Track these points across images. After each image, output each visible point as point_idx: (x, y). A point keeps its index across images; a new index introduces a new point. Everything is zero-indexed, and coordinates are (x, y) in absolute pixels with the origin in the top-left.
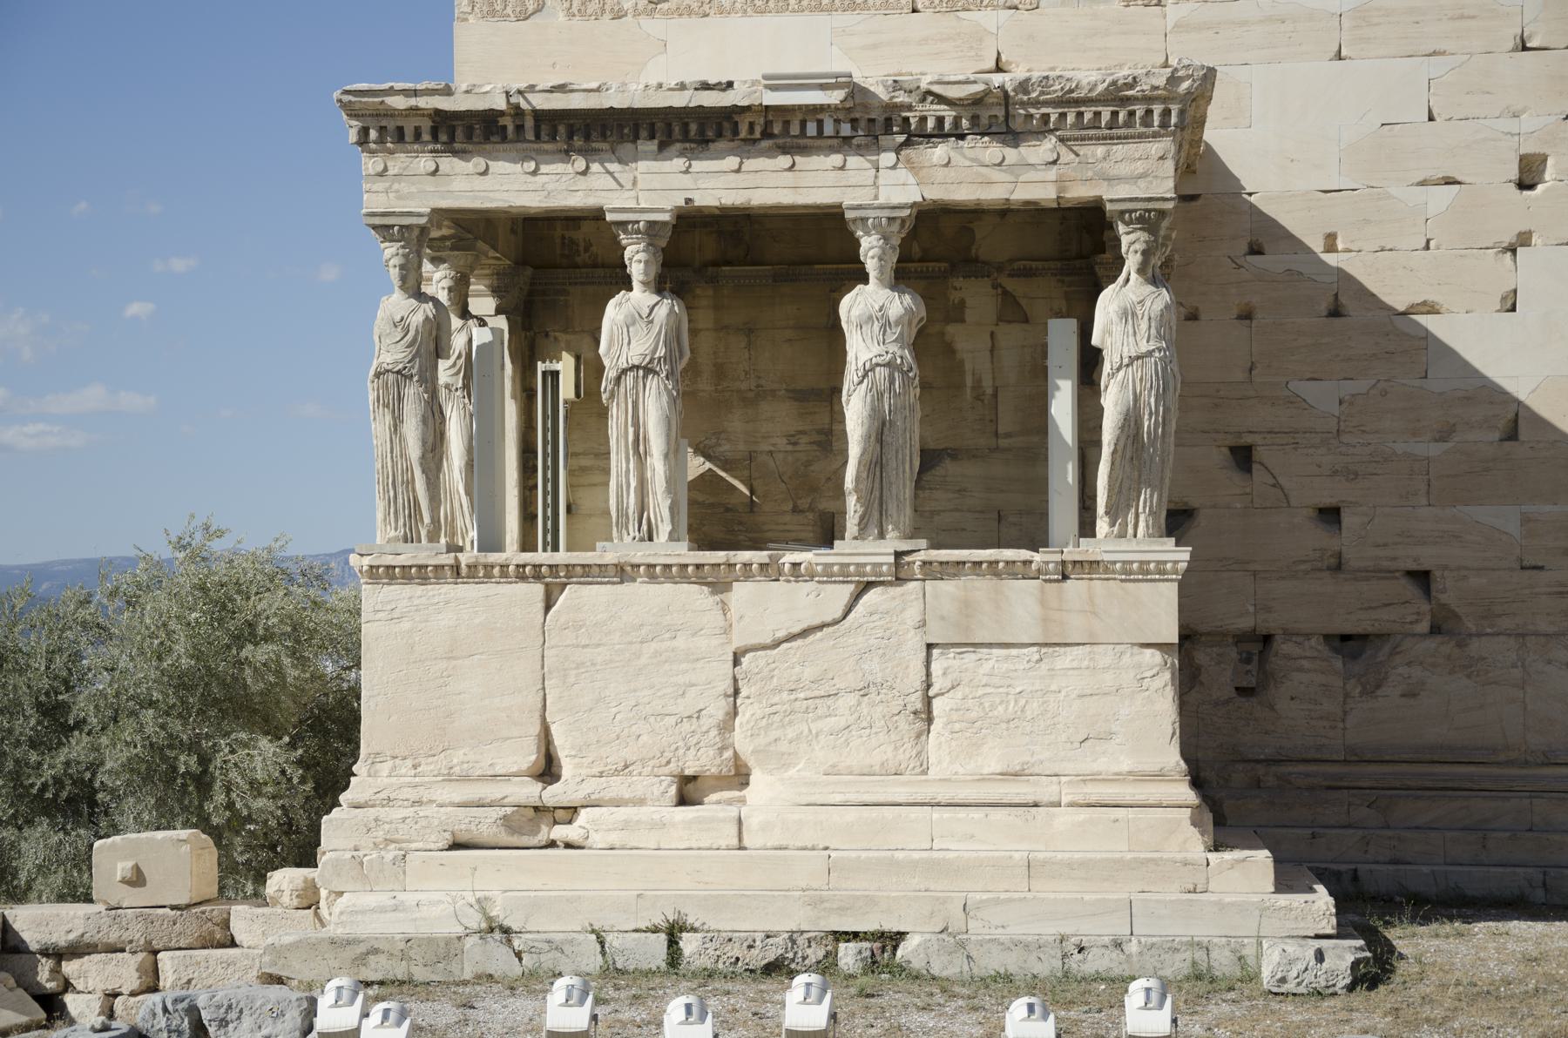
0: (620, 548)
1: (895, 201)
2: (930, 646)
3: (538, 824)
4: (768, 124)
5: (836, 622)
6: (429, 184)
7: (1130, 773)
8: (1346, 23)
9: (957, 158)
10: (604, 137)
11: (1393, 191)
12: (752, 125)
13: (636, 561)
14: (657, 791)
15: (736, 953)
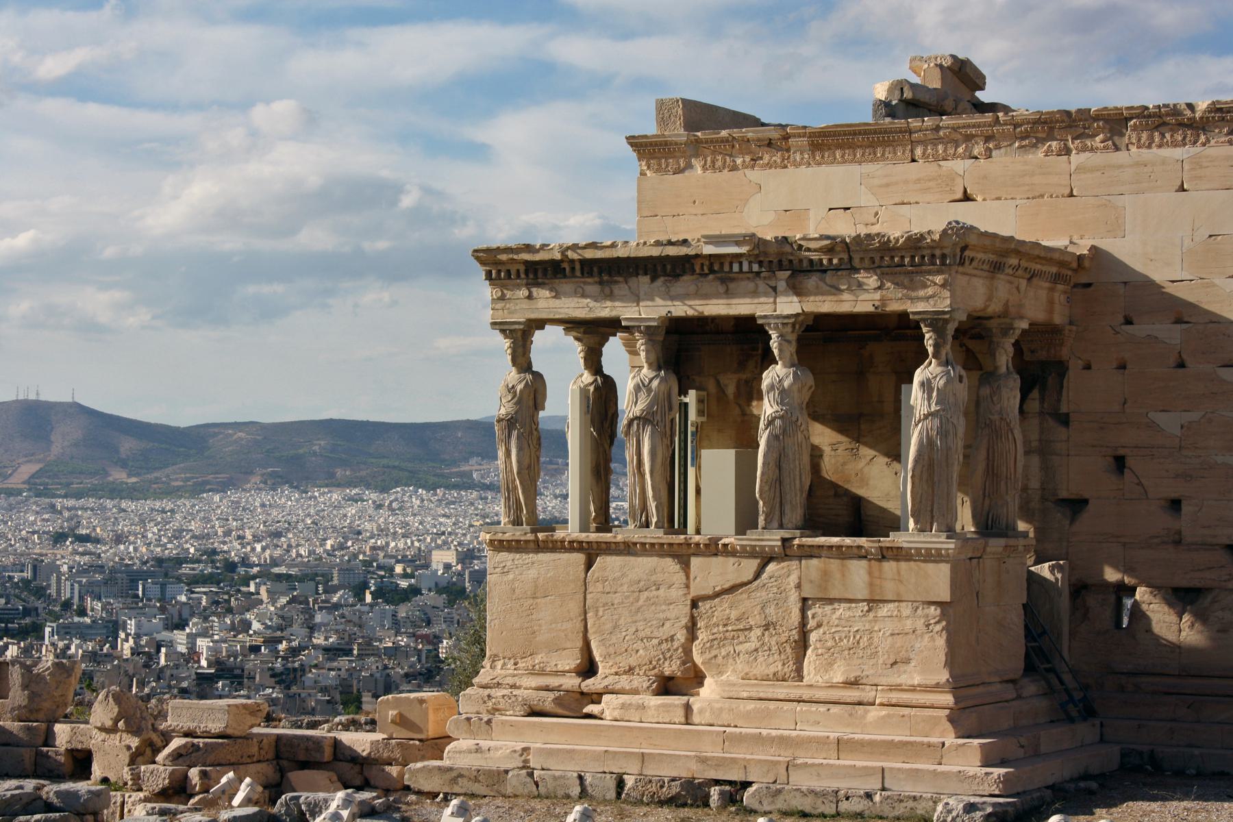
0: (630, 533)
1: (786, 313)
2: (804, 600)
3: (576, 704)
4: (711, 265)
5: (750, 582)
6: (525, 304)
7: (919, 685)
8: (1186, 167)
9: (821, 284)
10: (619, 274)
11: (1217, 281)
12: (702, 265)
13: (634, 540)
14: (646, 685)
15: (654, 789)
